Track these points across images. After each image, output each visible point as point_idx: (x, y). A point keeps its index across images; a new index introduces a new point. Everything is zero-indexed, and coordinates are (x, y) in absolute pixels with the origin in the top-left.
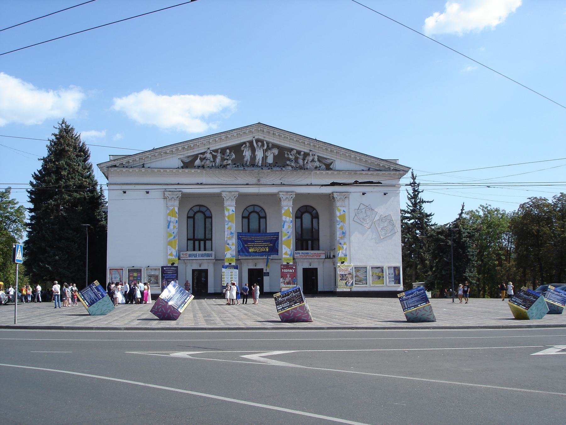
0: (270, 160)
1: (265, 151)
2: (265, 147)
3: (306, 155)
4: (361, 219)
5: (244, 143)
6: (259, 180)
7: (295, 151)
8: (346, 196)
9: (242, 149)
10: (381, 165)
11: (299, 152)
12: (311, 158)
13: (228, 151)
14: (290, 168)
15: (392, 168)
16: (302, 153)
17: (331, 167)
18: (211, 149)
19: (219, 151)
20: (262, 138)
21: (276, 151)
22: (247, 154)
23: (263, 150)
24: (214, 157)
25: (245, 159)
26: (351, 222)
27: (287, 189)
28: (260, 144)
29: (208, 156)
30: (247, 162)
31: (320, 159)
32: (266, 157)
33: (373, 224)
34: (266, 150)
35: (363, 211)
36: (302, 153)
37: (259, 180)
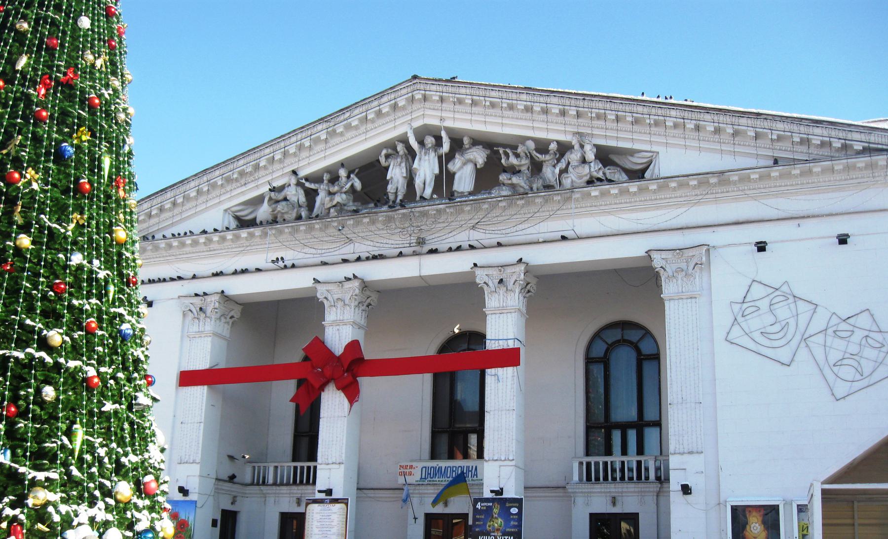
0: (464, 180)
1: (445, 160)
2: (446, 147)
3: (564, 148)
4: (757, 336)
5: (391, 145)
6: (421, 242)
7: (531, 145)
8: (699, 258)
9: (382, 160)
10: (816, 141)
11: (542, 146)
12: (574, 157)
13: (343, 173)
14: (505, 192)
15: (858, 147)
16: (553, 147)
17: (647, 175)
18: (302, 173)
19: (326, 177)
20: (435, 122)
21: (479, 156)
22: (396, 174)
23: (440, 158)
24: (311, 195)
25: (390, 188)
26: (721, 347)
27: (498, 255)
28: (430, 141)
29: (295, 195)
30: (396, 194)
31: (605, 156)
32: (451, 176)
33: (803, 353)
34: (450, 156)
35: (764, 304)
36: (553, 147)
37: (421, 242)
